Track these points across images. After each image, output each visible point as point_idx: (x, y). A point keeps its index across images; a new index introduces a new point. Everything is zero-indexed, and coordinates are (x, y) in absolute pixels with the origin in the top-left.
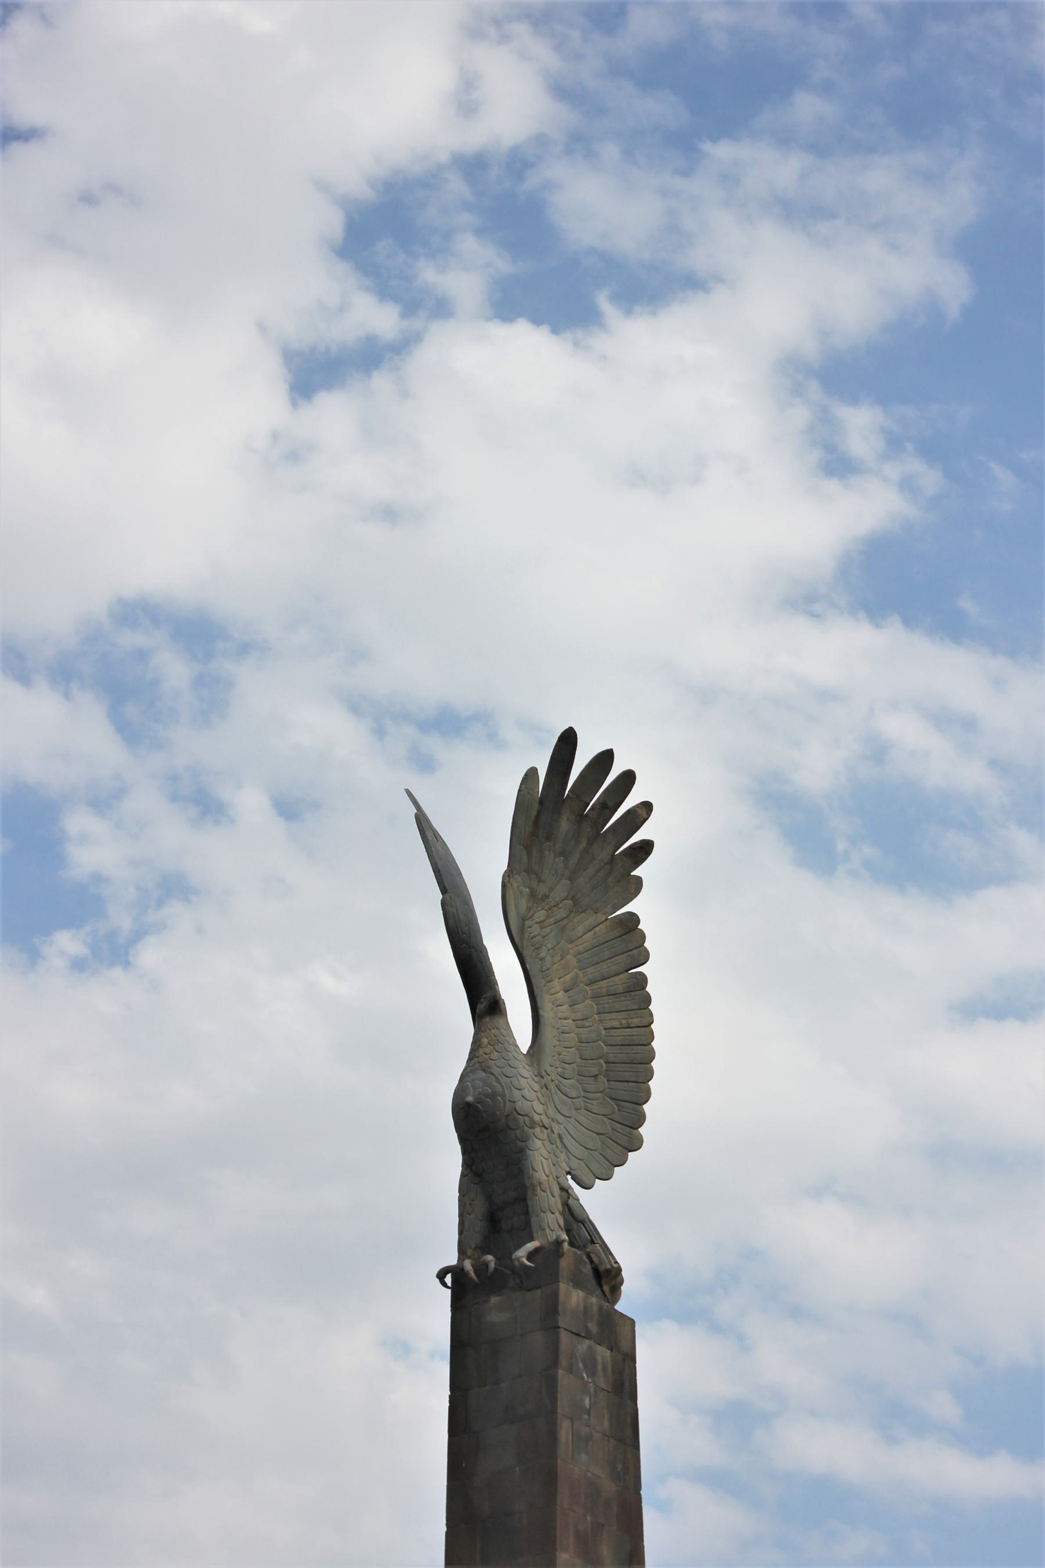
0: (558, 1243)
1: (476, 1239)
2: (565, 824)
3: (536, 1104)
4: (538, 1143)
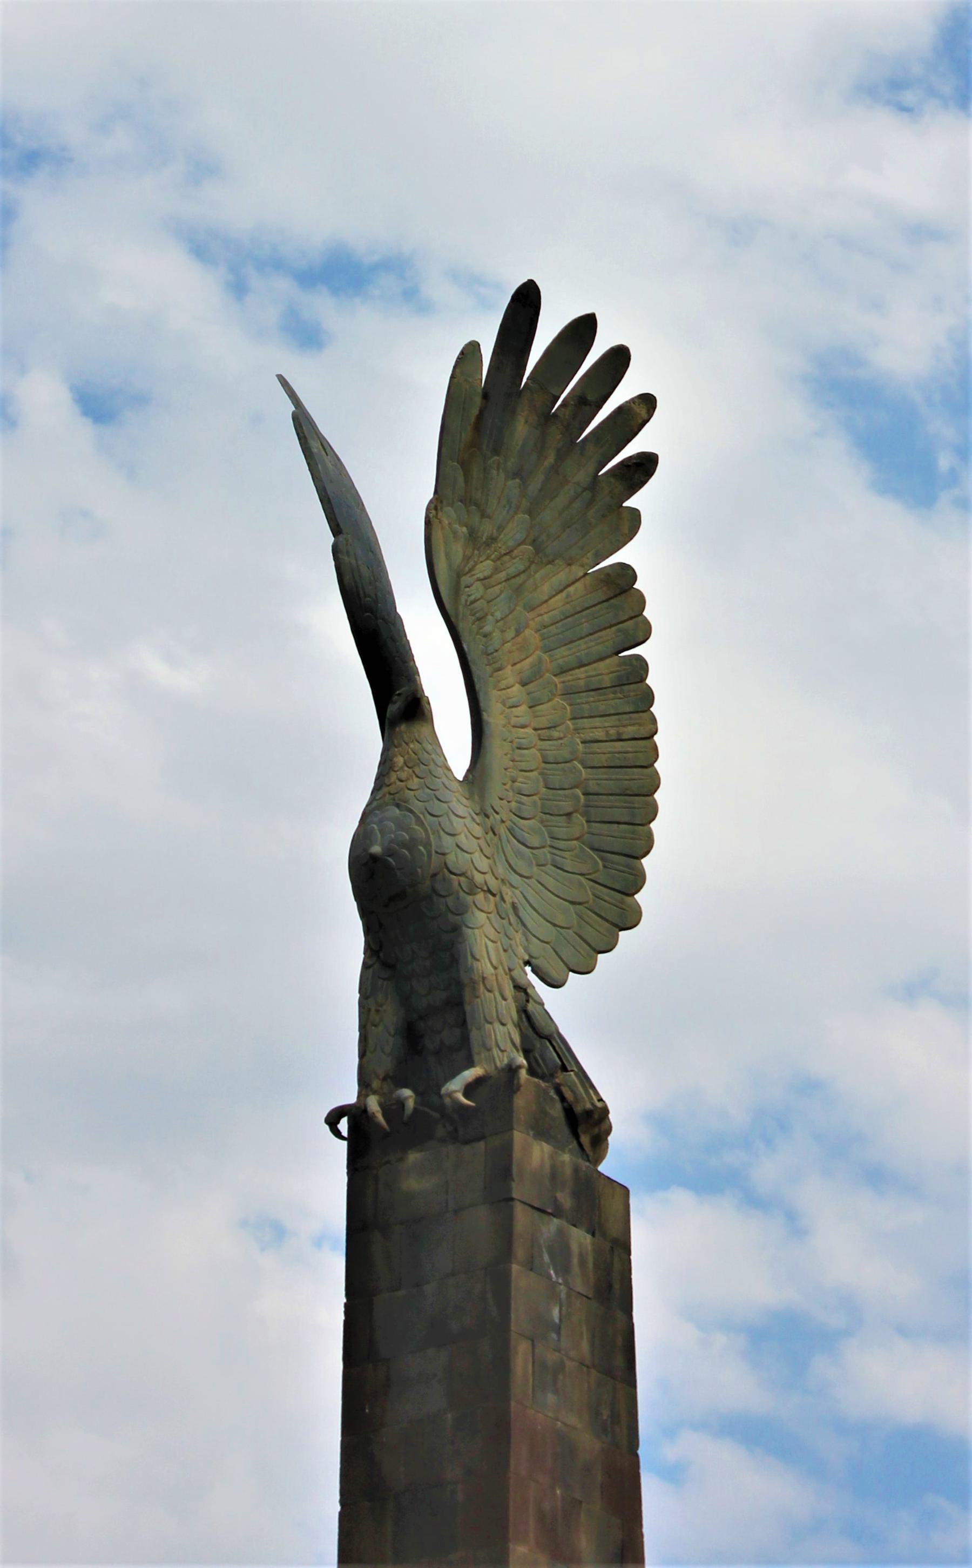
0: (512, 1070)
1: (385, 1064)
2: (522, 428)
3: (477, 857)
4: (481, 917)
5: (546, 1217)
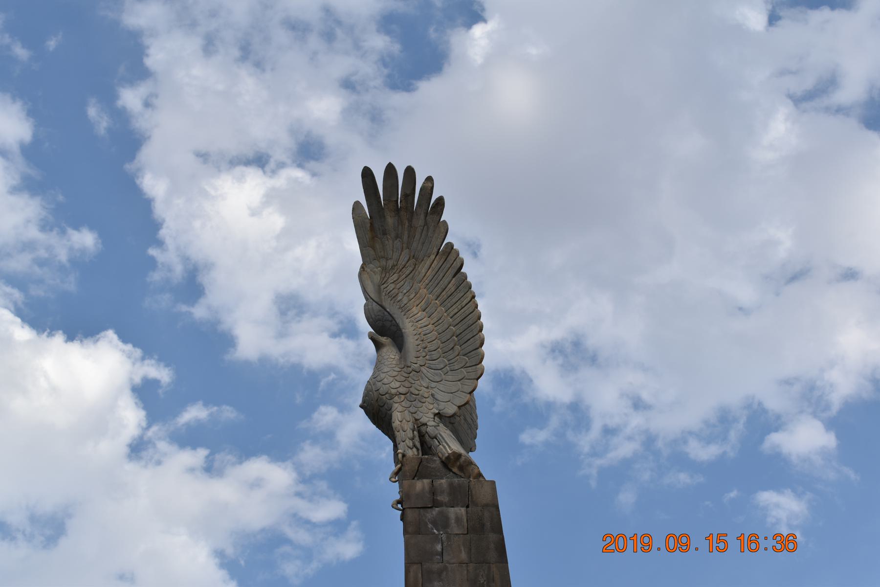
2: (390, 220)
4: (396, 405)
5: (429, 510)
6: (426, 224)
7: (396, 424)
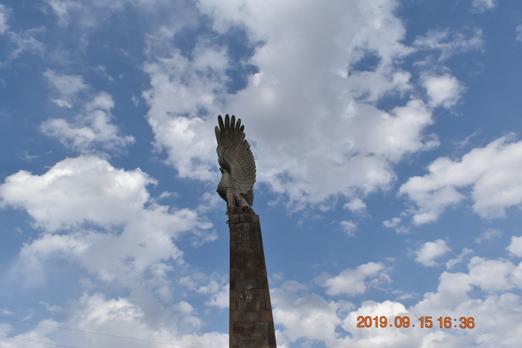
2: (227, 132)
6: (238, 133)
7: (228, 197)
